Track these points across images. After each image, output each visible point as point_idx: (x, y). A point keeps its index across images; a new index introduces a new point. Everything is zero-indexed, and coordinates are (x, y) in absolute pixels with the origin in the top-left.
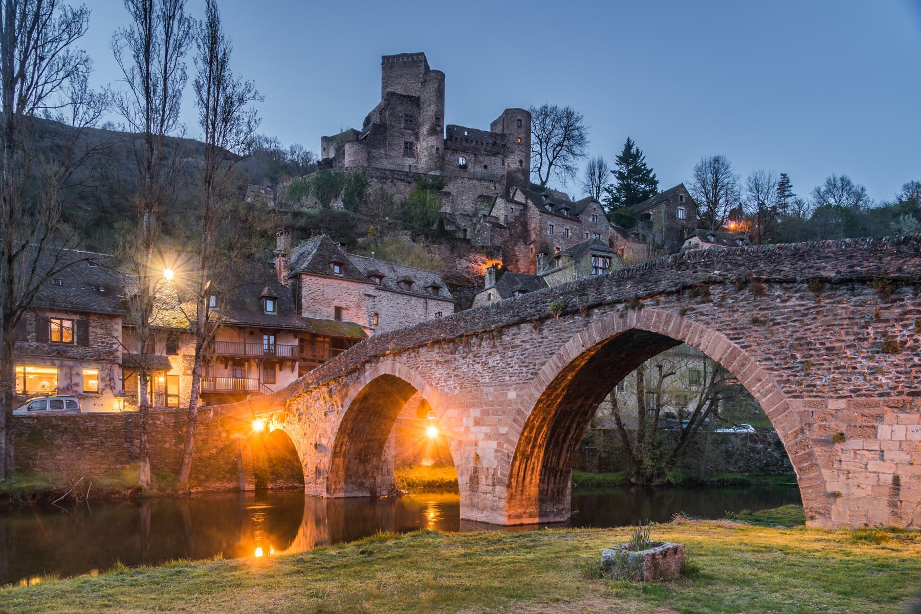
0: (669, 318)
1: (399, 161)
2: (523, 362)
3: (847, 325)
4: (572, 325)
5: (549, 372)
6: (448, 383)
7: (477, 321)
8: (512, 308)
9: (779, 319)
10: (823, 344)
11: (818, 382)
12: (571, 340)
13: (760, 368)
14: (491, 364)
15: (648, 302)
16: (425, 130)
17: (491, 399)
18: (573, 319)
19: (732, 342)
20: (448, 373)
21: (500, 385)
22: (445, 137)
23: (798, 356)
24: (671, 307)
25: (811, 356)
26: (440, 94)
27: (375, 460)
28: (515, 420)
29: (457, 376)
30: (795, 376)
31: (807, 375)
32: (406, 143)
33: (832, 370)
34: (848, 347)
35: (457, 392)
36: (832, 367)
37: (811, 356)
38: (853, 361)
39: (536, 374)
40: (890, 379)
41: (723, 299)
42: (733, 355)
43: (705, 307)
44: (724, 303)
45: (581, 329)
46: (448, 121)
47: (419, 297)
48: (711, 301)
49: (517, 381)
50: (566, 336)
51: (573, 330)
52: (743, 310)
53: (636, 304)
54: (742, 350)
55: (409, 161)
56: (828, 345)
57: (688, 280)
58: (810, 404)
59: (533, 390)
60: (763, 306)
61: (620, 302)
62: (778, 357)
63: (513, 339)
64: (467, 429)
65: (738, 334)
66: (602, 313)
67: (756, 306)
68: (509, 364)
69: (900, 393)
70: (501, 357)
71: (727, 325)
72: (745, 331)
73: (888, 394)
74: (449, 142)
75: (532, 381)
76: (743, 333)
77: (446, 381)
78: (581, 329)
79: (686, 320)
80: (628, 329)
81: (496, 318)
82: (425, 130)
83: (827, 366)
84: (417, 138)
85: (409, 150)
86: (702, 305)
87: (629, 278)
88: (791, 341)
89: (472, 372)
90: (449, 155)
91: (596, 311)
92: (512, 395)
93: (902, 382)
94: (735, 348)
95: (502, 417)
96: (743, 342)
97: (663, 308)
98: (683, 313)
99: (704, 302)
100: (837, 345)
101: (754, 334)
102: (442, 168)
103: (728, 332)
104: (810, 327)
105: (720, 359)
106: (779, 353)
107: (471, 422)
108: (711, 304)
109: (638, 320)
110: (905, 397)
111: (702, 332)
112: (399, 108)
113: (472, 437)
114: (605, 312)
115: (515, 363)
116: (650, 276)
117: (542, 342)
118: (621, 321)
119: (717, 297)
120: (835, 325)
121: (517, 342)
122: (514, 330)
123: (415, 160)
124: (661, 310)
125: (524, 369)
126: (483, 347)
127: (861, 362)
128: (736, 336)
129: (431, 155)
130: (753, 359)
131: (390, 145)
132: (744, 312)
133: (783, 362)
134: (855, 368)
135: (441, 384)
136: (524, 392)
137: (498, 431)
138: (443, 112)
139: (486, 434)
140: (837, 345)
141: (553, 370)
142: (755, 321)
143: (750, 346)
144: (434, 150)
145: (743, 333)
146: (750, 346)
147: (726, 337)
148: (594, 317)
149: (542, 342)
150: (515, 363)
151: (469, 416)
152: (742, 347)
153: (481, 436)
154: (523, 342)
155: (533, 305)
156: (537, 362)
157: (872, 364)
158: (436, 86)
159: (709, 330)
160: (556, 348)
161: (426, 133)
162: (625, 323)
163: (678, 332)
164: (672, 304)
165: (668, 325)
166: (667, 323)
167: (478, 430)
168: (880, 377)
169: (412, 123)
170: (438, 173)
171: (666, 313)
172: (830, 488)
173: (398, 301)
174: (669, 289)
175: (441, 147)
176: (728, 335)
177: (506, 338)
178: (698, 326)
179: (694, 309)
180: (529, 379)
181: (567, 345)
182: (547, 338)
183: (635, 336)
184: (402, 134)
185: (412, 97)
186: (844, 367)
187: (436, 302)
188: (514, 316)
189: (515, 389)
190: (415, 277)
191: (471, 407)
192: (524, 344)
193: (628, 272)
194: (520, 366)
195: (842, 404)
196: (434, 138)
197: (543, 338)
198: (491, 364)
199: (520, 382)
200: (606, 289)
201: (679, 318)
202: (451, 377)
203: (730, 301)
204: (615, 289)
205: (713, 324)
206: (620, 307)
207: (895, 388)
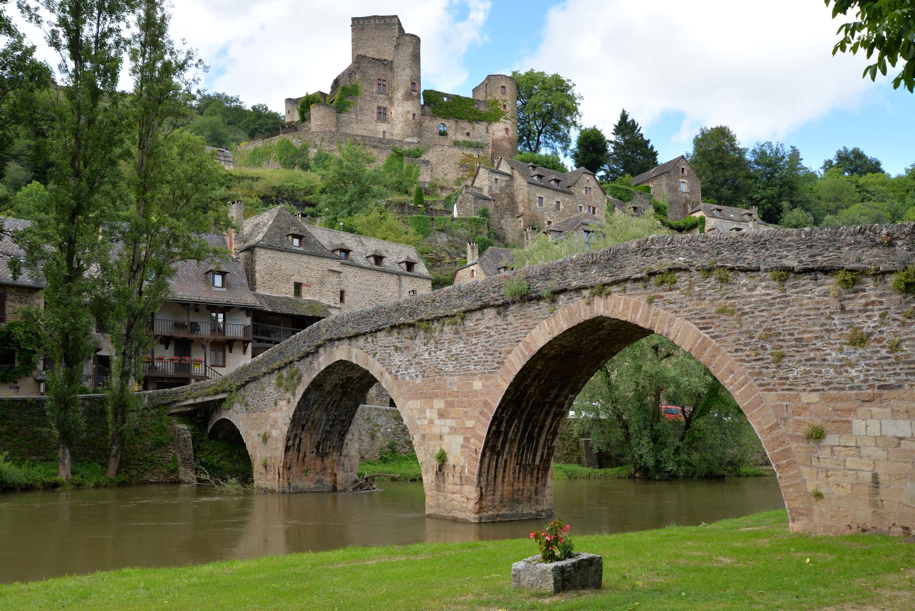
0: (637, 306)
1: (372, 126)
2: (488, 350)
3: (814, 315)
4: (538, 311)
5: (516, 362)
6: (410, 371)
7: (438, 304)
8: (474, 291)
9: (747, 308)
10: (791, 334)
11: (791, 375)
12: (537, 327)
13: (731, 359)
15: (614, 288)
16: (399, 94)
17: (455, 389)
18: (538, 305)
19: (702, 332)
20: (409, 360)
21: (464, 374)
22: (422, 103)
23: (768, 346)
24: (637, 295)
25: (781, 347)
26: (416, 57)
27: (335, 454)
28: (481, 413)
29: (419, 363)
30: (767, 368)
31: (779, 366)
32: (379, 108)
33: (804, 362)
34: (816, 338)
35: (418, 381)
36: (803, 359)
37: (781, 347)
38: (822, 353)
39: (503, 363)
40: (861, 371)
41: (690, 286)
42: (704, 346)
43: (675, 294)
44: (691, 291)
45: (547, 315)
46: (425, 86)
47: (392, 273)
48: (678, 289)
49: (482, 371)
50: (532, 323)
51: (539, 317)
52: (711, 298)
53: (602, 290)
54: (713, 340)
55: (383, 127)
56: (797, 336)
57: (653, 266)
58: (783, 398)
59: (499, 380)
60: (731, 295)
61: (585, 288)
62: (748, 348)
63: (476, 325)
64: (431, 422)
65: (707, 323)
66: (568, 299)
67: (723, 295)
68: (473, 352)
69: (871, 386)
70: (465, 343)
71: (696, 314)
72: (714, 321)
73: (859, 388)
74: (426, 108)
75: (498, 371)
76: (712, 323)
77: (406, 369)
78: (547, 315)
79: (654, 307)
80: (595, 316)
81: (458, 302)
82: (399, 94)
83: (798, 358)
84: (392, 103)
85: (382, 114)
86: (669, 293)
87: (593, 263)
88: (760, 331)
89: (434, 360)
90: (427, 122)
91: (562, 296)
92: (477, 385)
93: (872, 375)
94: (705, 338)
95: (468, 409)
96: (713, 332)
97: (630, 295)
98: (650, 301)
99: (671, 290)
100: (806, 336)
101: (725, 324)
102: (419, 135)
103: (698, 321)
104: (777, 317)
105: (691, 349)
106: (749, 344)
108: (678, 292)
110: (876, 391)
111: (672, 320)
112: (371, 72)
113: (436, 430)
114: (572, 298)
115: (480, 351)
116: (615, 262)
117: (507, 329)
118: (588, 307)
119: (683, 285)
120: (801, 315)
121: (481, 328)
122: (478, 315)
123: (389, 126)
124: (628, 297)
125: (490, 358)
126: (445, 333)
127: (830, 354)
128: (705, 326)
129: (407, 120)
130: (724, 349)
131: (361, 109)
132: (711, 301)
133: (753, 353)
134: (824, 360)
135: (401, 372)
136: (489, 383)
137: (464, 424)
138: (419, 77)
139: (451, 428)
140: (806, 336)
141: (519, 358)
142: (722, 311)
143: (720, 336)
144: (410, 116)
145: (712, 323)
146: (720, 336)
147: (694, 326)
148: (560, 303)
149: (507, 329)
150: (480, 351)
151: (432, 408)
152: (713, 337)
153: (446, 430)
154: (487, 328)
155: (496, 289)
156: (503, 349)
157: (841, 356)
158: (411, 50)
159: (678, 319)
160: (523, 335)
161: (401, 98)
162: (592, 310)
163: (646, 321)
164: (639, 291)
165: (637, 313)
167: (443, 423)
168: (850, 369)
169: (384, 86)
170: (415, 140)
171: (633, 300)
173: (367, 277)
174: (634, 276)
175: (418, 112)
176: (697, 324)
177: (469, 324)
178: (666, 315)
179: (661, 297)
180: (495, 369)
181: (533, 332)
182: (512, 325)
183: (605, 324)
184: (375, 98)
185: (385, 60)
186: (814, 359)
187: (410, 279)
188: (477, 301)
189: (480, 379)
190: (387, 251)
191: (434, 398)
192: (488, 331)
193: (592, 256)
194: (485, 354)
195: (815, 397)
196: (410, 103)
197: (508, 324)
198: (454, 351)
199: (486, 371)
200: (570, 273)
201: (647, 305)
202: (412, 364)
203: (697, 289)
204: (579, 274)
205: (681, 313)
206: (586, 293)
207: (865, 381)
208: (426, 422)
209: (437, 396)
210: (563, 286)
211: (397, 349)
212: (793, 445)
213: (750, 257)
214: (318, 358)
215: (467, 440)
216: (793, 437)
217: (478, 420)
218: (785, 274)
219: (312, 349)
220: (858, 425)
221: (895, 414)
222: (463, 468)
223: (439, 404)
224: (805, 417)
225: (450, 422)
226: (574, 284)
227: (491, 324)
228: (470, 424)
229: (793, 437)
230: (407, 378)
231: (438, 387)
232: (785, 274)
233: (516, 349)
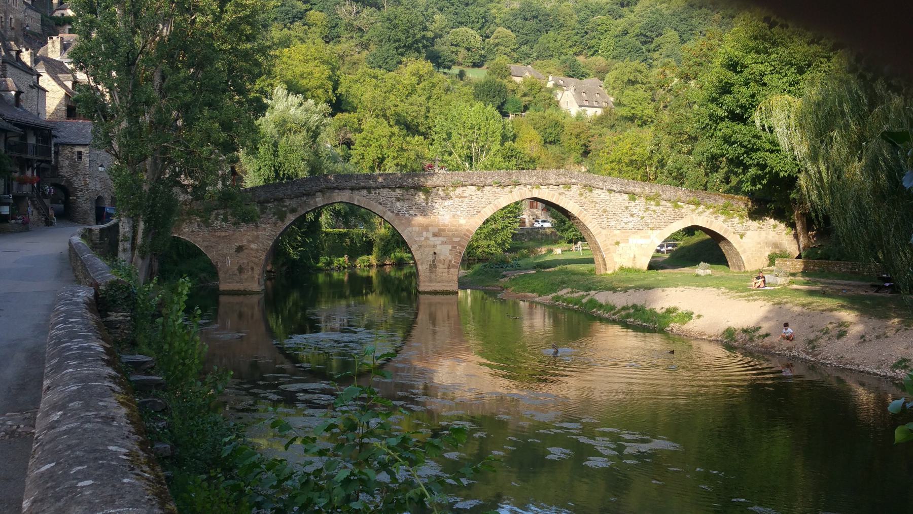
42: (581, 213)
59: (477, 220)
79: (561, 197)
109: (539, 194)
113: (432, 243)
121: (465, 195)
166: (552, 197)
214: (315, 198)
215: (454, 247)
216: (611, 244)
218: (611, 191)
220: (630, 240)
221: (641, 237)
222: (450, 261)
225: (441, 239)
227: (473, 193)
229: (611, 244)
230: (407, 215)
233: (489, 206)
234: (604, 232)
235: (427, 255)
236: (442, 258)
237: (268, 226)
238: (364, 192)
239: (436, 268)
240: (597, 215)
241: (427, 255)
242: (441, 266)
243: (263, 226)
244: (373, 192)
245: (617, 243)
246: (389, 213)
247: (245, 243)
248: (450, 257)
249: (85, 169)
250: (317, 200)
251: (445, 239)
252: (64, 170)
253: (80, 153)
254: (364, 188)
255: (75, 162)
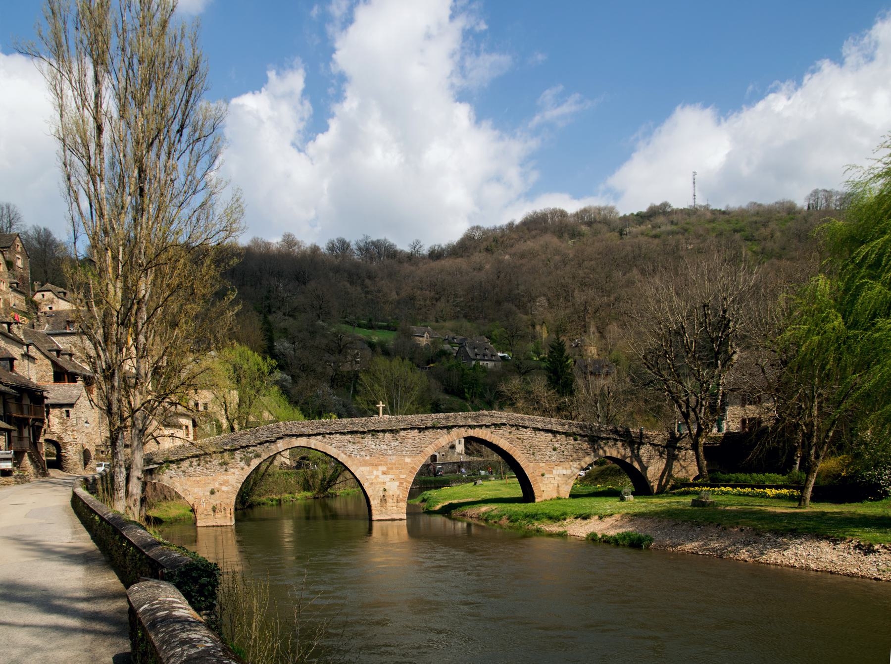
13: (520, 453)
14: (393, 445)
35: (368, 458)
42: (511, 449)
53: (472, 427)
59: (421, 458)
79: (493, 435)
107: (380, 473)
113: (380, 480)
166: (486, 435)
171: (485, 432)
172: (542, 489)
195: (544, 464)
198: (393, 445)
208: (373, 477)
209: (381, 465)
210: (455, 424)
211: (350, 442)
212: (538, 478)
213: (527, 423)
215: (401, 483)
217: (408, 475)
219: (273, 439)
220: (554, 472)
222: (399, 496)
223: (384, 469)
224: (541, 470)
226: (461, 424)
228: (404, 476)
230: (358, 457)
231: (381, 461)
232: (536, 429)
233: (430, 446)
234: (531, 465)
235: (378, 491)
236: (391, 493)
237: (236, 470)
238: (320, 437)
239: (386, 502)
240: (525, 451)
241: (378, 491)
242: (390, 501)
243: (232, 470)
244: (327, 436)
245: (543, 475)
246: (342, 455)
247: (217, 485)
248: (398, 492)
249: (73, 426)
250: (278, 445)
251: (393, 477)
252: (55, 427)
253: (68, 412)
254: (319, 434)
255: (64, 420)
